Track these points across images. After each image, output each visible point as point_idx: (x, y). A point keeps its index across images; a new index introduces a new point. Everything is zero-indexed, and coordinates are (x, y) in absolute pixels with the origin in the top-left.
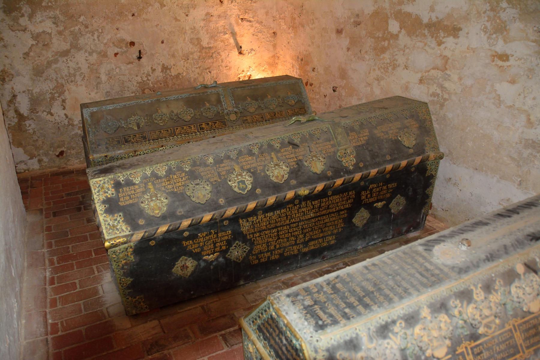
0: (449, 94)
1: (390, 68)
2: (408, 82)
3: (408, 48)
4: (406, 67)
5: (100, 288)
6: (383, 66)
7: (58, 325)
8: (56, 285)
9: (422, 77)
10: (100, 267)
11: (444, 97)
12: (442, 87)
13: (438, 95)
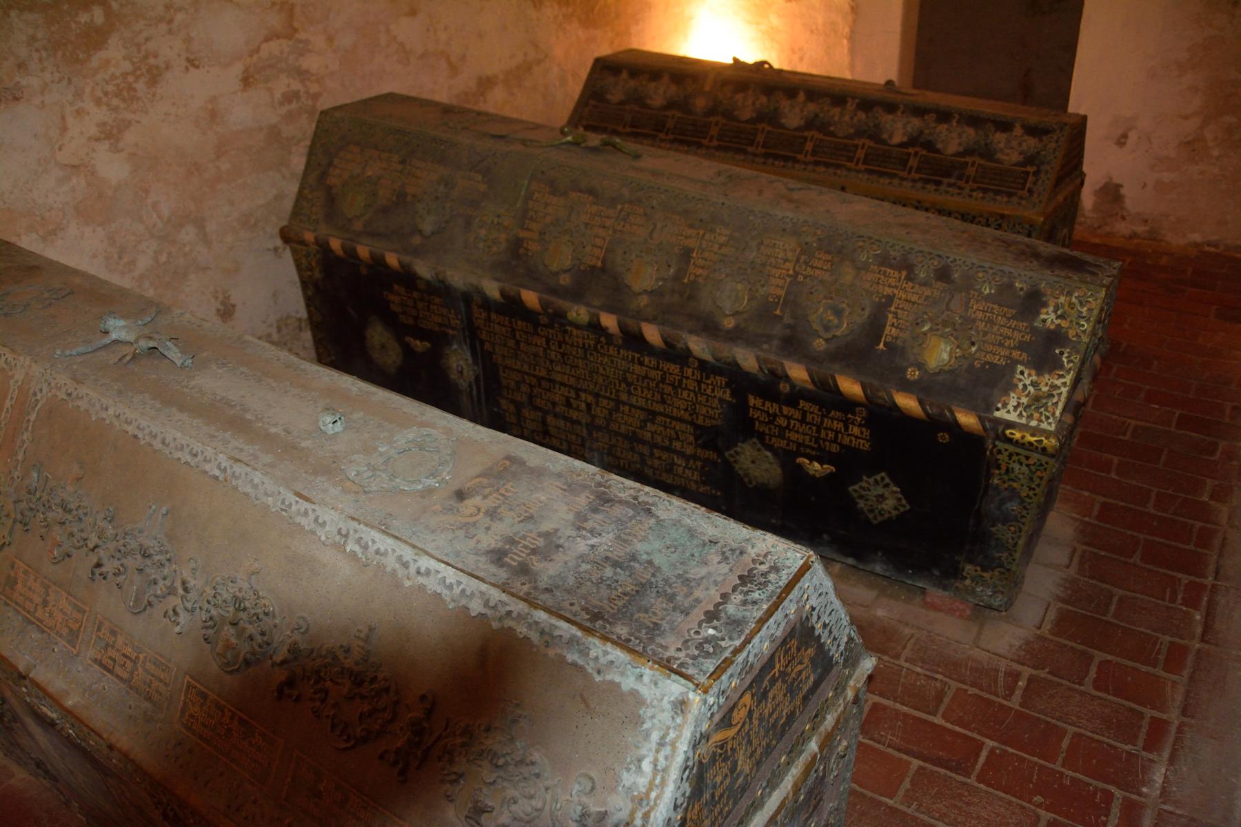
1: (140, 86)
2: (213, 99)
3: (180, 9)
4: (192, 63)
5: (1047, 626)
6: (111, 88)
7: (1183, 599)
8: (1149, 713)
9: (246, 70)
10: (1001, 691)
11: (311, 91)
12: (302, 75)
13: (296, 95)
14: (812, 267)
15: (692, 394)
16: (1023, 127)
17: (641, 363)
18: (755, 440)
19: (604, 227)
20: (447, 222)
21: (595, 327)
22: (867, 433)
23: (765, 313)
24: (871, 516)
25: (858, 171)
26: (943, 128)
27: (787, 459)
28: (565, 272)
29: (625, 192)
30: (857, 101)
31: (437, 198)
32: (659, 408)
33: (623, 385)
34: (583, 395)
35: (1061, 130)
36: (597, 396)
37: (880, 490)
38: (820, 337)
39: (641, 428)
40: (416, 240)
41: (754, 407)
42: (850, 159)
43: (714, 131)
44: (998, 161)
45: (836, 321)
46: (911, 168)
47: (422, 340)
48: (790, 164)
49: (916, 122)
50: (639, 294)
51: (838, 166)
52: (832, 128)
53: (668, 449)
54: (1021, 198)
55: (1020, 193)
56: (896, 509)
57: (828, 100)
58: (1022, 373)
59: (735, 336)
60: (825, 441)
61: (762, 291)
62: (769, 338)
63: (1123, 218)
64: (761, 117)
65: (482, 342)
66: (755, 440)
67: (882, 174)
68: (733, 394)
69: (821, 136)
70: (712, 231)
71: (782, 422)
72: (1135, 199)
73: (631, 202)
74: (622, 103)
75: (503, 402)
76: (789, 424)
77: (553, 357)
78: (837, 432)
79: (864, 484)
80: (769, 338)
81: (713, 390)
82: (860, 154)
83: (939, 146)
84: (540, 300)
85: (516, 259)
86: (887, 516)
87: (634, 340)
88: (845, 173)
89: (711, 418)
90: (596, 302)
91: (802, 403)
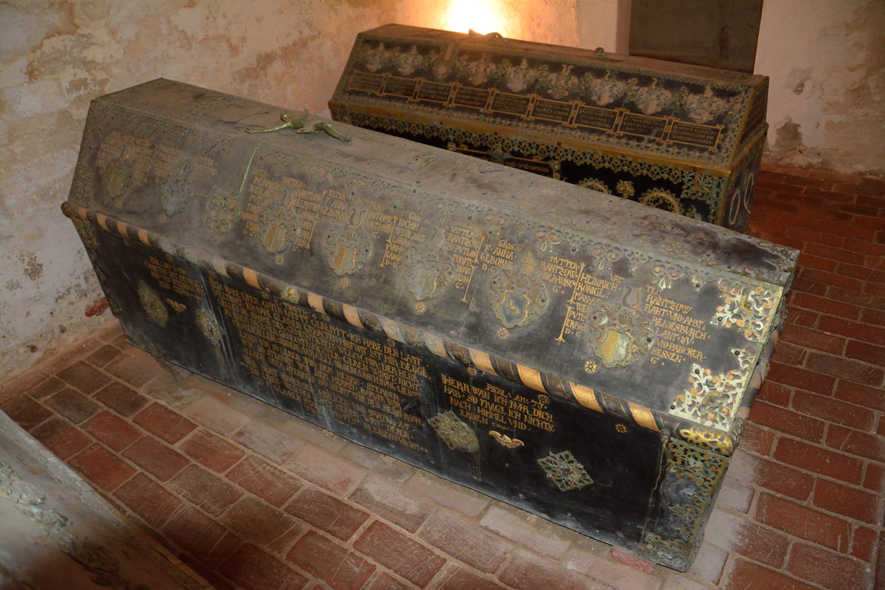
0: (103, 69)
7: (854, 548)
9: (30, 64)
11: (98, 78)
12: (89, 65)
13: (84, 82)
14: (496, 257)
15: (394, 369)
16: (713, 89)
17: (348, 339)
18: (451, 412)
19: (312, 211)
20: (186, 203)
21: (304, 303)
22: (550, 417)
23: (453, 300)
24: (559, 485)
25: (572, 129)
26: (644, 90)
27: (482, 429)
28: (280, 253)
29: (330, 177)
30: (571, 67)
31: (178, 181)
32: (369, 377)
33: (337, 355)
34: (306, 359)
35: (746, 92)
36: (317, 361)
37: (565, 465)
38: (503, 326)
39: (356, 391)
40: (163, 219)
41: (447, 385)
42: (565, 118)
43: (453, 95)
44: (691, 120)
45: (518, 311)
46: (617, 126)
47: (179, 303)
48: (514, 123)
49: (621, 86)
50: (342, 276)
51: (556, 125)
52: (550, 92)
53: (380, 411)
54: (711, 153)
55: (711, 148)
56: (580, 481)
57: (546, 67)
58: (697, 372)
59: (425, 321)
60: (512, 419)
61: (451, 279)
62: (457, 324)
63: (801, 152)
64: (491, 83)
65: (223, 312)
66: (451, 412)
67: (592, 131)
68: (428, 371)
69: (540, 98)
70: (405, 218)
71: (474, 400)
72: (809, 136)
73: (335, 188)
74: (379, 71)
75: (247, 358)
76: (479, 402)
77: (278, 326)
78: (523, 414)
79: (549, 458)
80: (457, 324)
81: (411, 367)
82: (574, 114)
83: (641, 107)
84: (259, 279)
85: (241, 239)
86: (573, 486)
87: (339, 319)
88: (560, 130)
89: (411, 390)
90: (305, 283)
91: (489, 387)
